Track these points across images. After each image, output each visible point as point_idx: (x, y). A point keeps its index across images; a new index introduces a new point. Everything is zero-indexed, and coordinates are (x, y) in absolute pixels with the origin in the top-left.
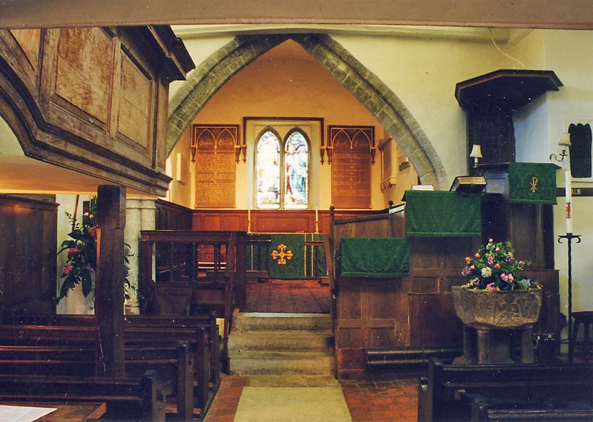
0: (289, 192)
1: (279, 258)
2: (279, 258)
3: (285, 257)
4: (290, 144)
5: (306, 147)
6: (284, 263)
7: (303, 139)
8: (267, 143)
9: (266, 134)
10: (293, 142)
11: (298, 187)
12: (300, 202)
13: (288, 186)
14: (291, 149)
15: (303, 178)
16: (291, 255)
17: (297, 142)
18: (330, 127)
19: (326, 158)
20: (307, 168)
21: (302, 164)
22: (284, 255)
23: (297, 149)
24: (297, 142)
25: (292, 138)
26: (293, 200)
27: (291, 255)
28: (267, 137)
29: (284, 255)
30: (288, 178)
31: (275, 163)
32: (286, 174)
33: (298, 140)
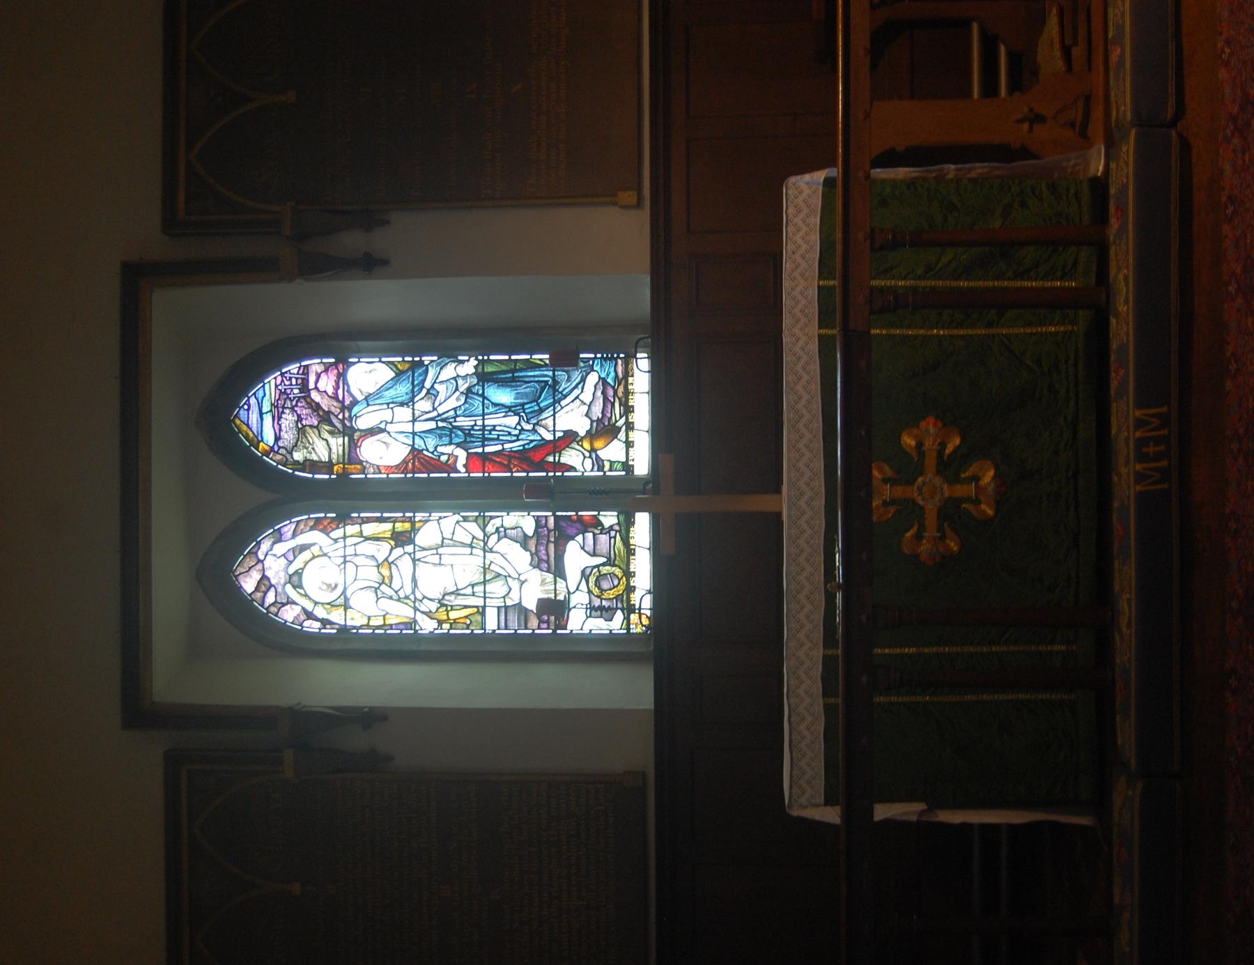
0: (572, 457)
1: (951, 513)
2: (951, 513)
3: (950, 467)
4: (298, 456)
5: (315, 365)
6: (988, 476)
7: (270, 387)
8: (295, 579)
9: (249, 584)
10: (288, 437)
11: (529, 410)
12: (616, 392)
13: (526, 457)
14: (325, 447)
15: (483, 377)
16: (930, 426)
17: (288, 419)
18: (171, 224)
19: (352, 241)
20: (426, 359)
21: (403, 389)
22: (929, 477)
23: (325, 417)
24: (288, 419)
25: (269, 437)
26: (604, 430)
27: (930, 426)
28: (264, 583)
29: (929, 477)
30: (484, 457)
31: (401, 539)
32: (463, 474)
33: (278, 413)
